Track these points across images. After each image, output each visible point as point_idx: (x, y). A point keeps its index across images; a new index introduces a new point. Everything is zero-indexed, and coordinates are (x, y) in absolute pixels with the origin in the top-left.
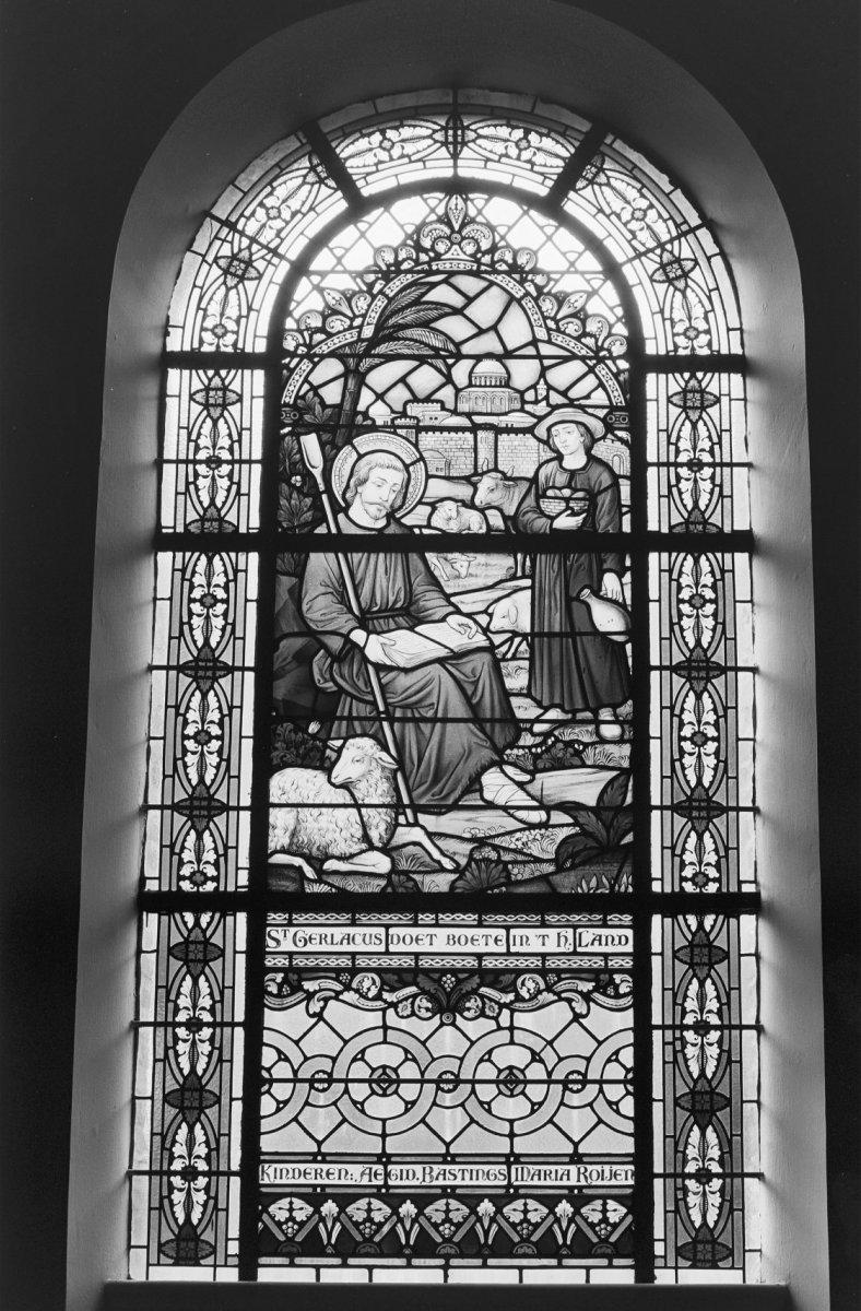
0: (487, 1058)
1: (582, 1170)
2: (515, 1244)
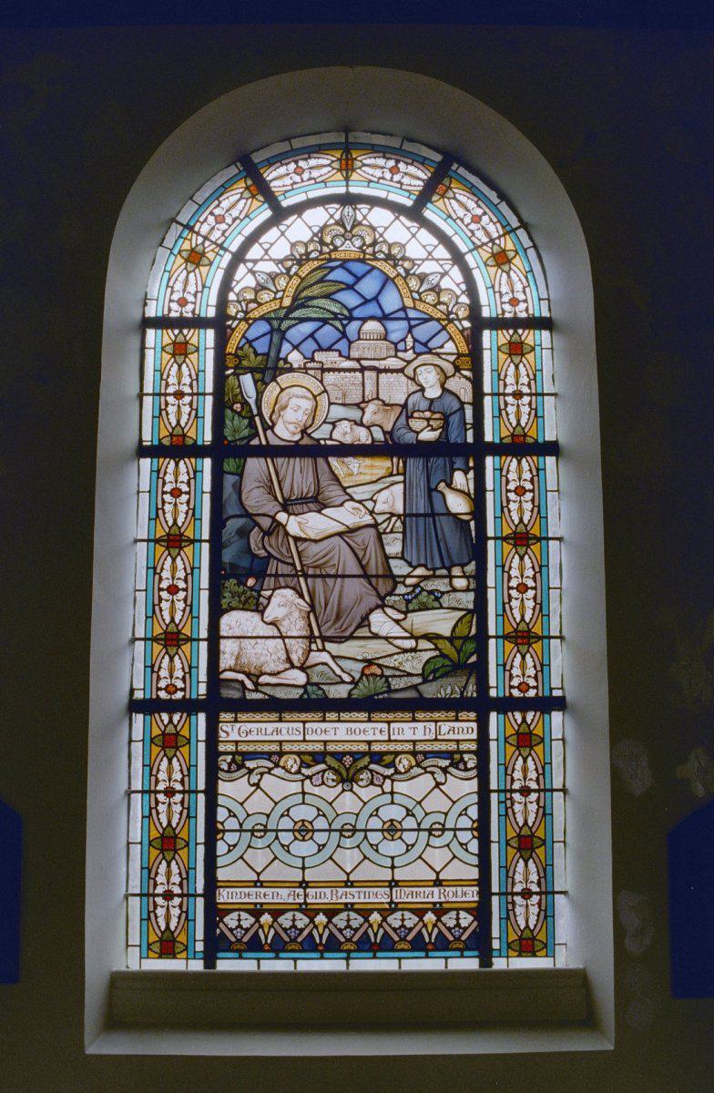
0: (375, 813)
1: (442, 891)
2: (396, 943)
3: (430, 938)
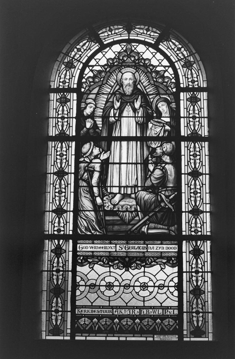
0: (103, 279)
1: (148, 311)
3: (137, 329)
